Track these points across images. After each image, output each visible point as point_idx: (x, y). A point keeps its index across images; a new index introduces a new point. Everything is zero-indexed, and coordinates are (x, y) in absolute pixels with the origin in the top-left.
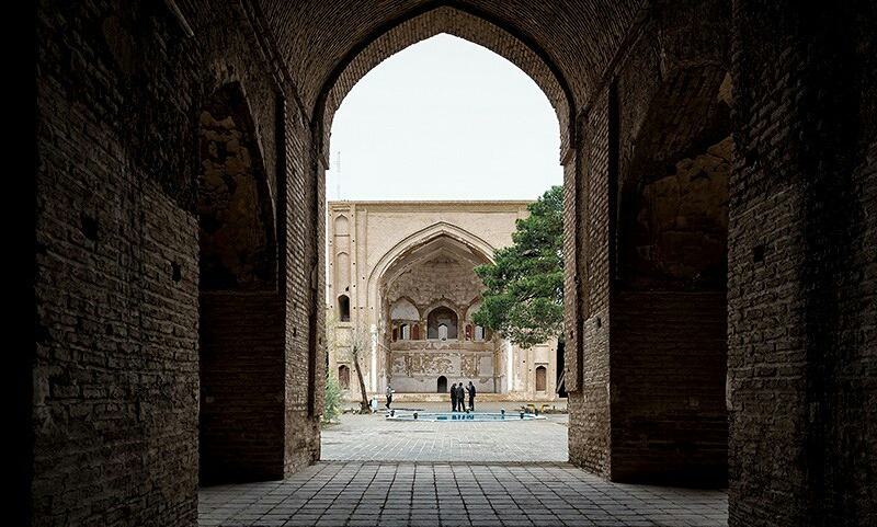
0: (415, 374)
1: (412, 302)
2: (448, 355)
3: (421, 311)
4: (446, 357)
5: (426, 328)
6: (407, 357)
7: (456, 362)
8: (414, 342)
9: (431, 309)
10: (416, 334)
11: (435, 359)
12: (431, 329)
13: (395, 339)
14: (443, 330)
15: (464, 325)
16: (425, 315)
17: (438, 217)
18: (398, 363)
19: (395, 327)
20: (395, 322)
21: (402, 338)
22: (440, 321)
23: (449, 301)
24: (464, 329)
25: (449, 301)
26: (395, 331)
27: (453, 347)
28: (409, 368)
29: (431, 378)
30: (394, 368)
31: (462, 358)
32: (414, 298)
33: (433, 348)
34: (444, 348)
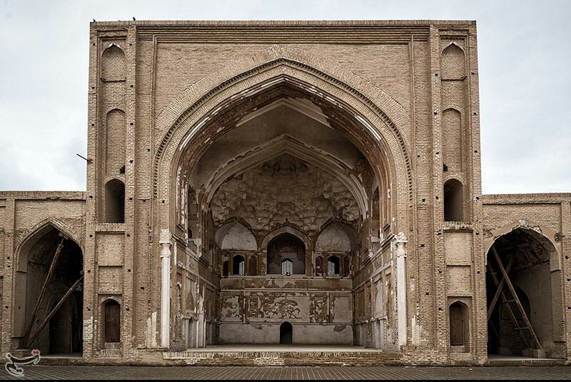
0: (251, 319)
1: (247, 226)
2: (293, 294)
3: (259, 239)
4: (290, 298)
5: (265, 260)
6: (241, 297)
7: (304, 304)
8: (249, 278)
9: (271, 237)
10: (253, 269)
11: (277, 300)
12: (273, 265)
13: (226, 274)
14: (287, 267)
15: (314, 257)
16: (265, 244)
17: (275, 52)
18: (230, 305)
19: (225, 259)
20: (227, 252)
21: (236, 272)
22: (285, 255)
23: (294, 226)
24: (314, 262)
25: (294, 226)
26: (226, 264)
27: (300, 285)
28: (244, 311)
29: (270, 324)
30: (224, 311)
31: (312, 299)
32: (251, 222)
33: (274, 286)
34: (289, 286)
